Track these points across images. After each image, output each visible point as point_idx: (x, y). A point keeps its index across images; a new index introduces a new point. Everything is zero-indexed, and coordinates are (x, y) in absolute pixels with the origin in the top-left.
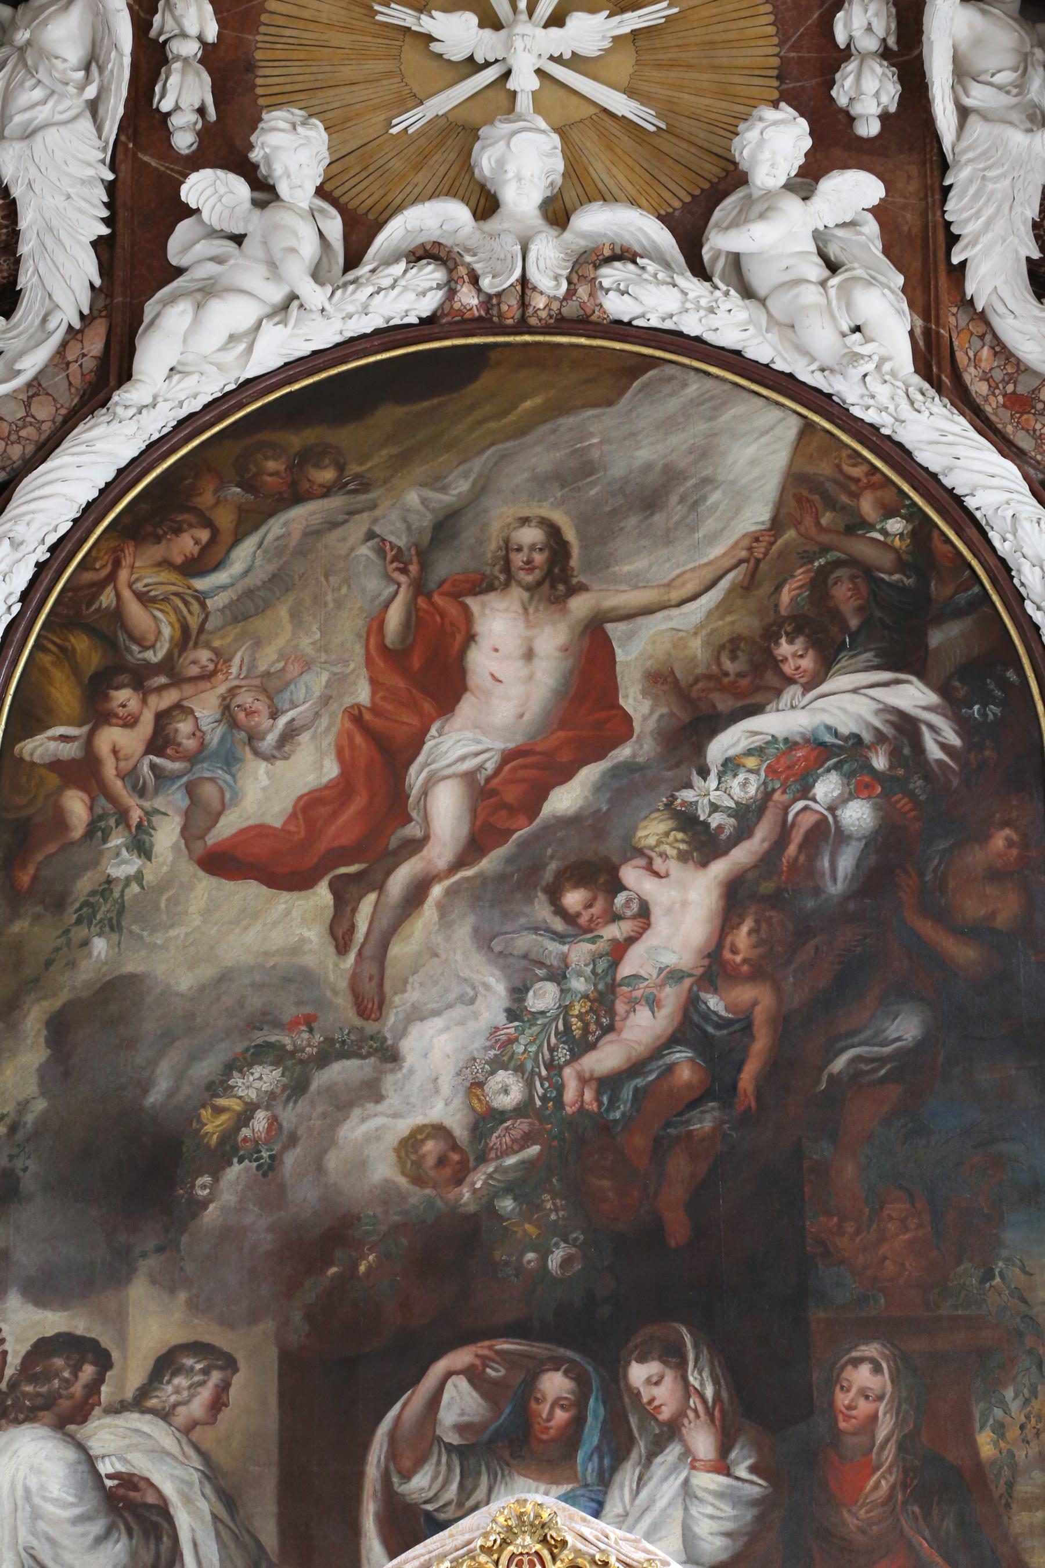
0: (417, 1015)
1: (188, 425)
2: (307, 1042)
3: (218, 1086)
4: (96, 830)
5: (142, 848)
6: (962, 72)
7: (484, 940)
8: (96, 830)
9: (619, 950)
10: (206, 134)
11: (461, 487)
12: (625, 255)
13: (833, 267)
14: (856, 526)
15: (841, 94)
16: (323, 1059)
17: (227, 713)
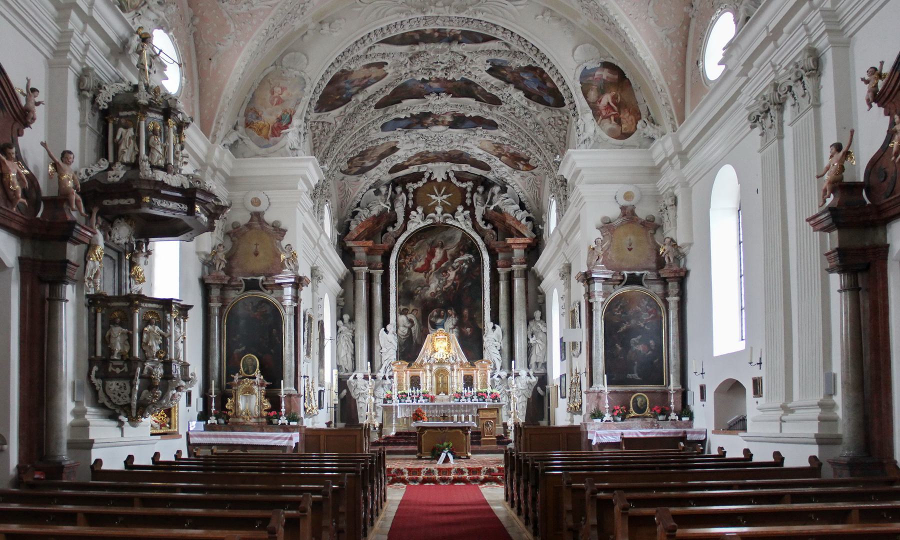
0: (431, 283)
1: (412, 233)
2: (423, 285)
3: (416, 289)
4: (406, 268)
5: (409, 269)
6: (477, 201)
7: (437, 277)
8: (406, 268)
9: (447, 278)
10: (412, 206)
11: (434, 238)
12: (448, 218)
13: (465, 218)
14: (467, 241)
15: (466, 202)
16: (425, 286)
17: (416, 258)
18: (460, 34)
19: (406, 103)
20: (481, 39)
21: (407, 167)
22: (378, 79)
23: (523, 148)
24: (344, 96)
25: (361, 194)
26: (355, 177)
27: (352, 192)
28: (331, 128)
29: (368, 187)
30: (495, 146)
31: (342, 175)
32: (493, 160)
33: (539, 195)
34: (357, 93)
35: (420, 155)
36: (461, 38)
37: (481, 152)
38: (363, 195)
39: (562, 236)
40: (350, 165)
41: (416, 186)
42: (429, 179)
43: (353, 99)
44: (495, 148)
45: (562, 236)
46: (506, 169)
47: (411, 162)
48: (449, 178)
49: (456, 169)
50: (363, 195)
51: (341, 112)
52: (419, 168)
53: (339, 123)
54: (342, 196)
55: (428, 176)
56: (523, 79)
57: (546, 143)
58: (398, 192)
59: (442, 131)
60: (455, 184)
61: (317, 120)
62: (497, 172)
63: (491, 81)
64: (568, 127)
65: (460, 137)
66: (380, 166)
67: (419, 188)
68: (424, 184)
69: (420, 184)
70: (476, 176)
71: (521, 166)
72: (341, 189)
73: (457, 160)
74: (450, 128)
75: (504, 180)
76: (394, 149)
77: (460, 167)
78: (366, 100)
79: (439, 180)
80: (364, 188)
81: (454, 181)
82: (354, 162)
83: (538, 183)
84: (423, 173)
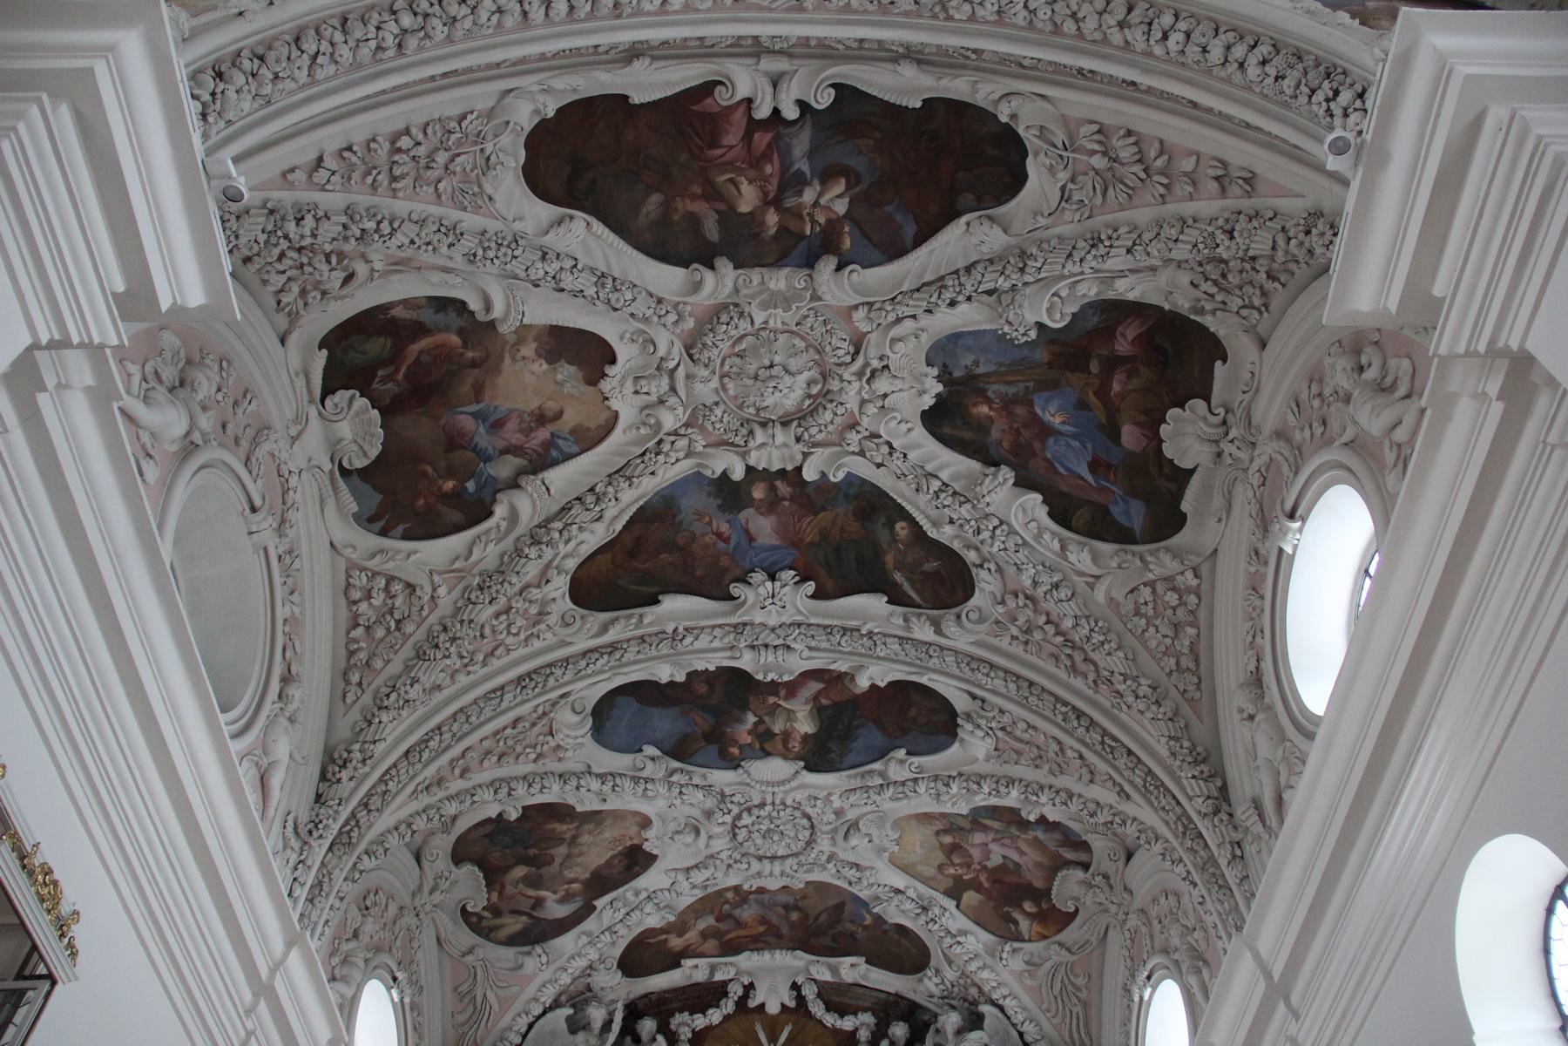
18: (848, 216)
19: (676, 607)
20: (910, 230)
21: (673, 962)
22: (588, 439)
23: (1042, 788)
24: (471, 486)
25: (523, 1023)
26: (508, 953)
27: (496, 1007)
28: (414, 610)
29: (547, 999)
30: (942, 845)
31: (467, 937)
32: (937, 911)
33: (1087, 1026)
34: (514, 484)
35: (712, 903)
36: (847, 243)
37: (900, 881)
38: (531, 1026)
39: (1268, 975)
40: (495, 896)
41: (700, 1022)
42: (742, 1002)
43: (500, 511)
44: (940, 857)
45: (1268, 975)
46: (978, 940)
47: (692, 936)
48: (801, 999)
49: (826, 976)
50: (531, 1026)
51: (457, 558)
52: (713, 969)
53: (442, 591)
54: (463, 1017)
55: (740, 992)
56: (1046, 431)
57: (1135, 679)
58: (645, 1036)
59: (783, 783)
60: (820, 1022)
61: (371, 564)
62: (950, 962)
63: (942, 467)
64: (1202, 614)
65: (839, 813)
66: (590, 924)
67: (709, 1028)
68: (727, 1018)
69: (715, 1016)
70: (883, 996)
71: (1024, 925)
72: (464, 988)
73: (826, 941)
74: (810, 768)
75: (973, 991)
76: (636, 860)
77: (834, 970)
78: (539, 526)
79: (773, 1008)
80: (537, 1000)
81: (817, 1009)
82: (510, 890)
83: (1080, 981)
84: (725, 983)
